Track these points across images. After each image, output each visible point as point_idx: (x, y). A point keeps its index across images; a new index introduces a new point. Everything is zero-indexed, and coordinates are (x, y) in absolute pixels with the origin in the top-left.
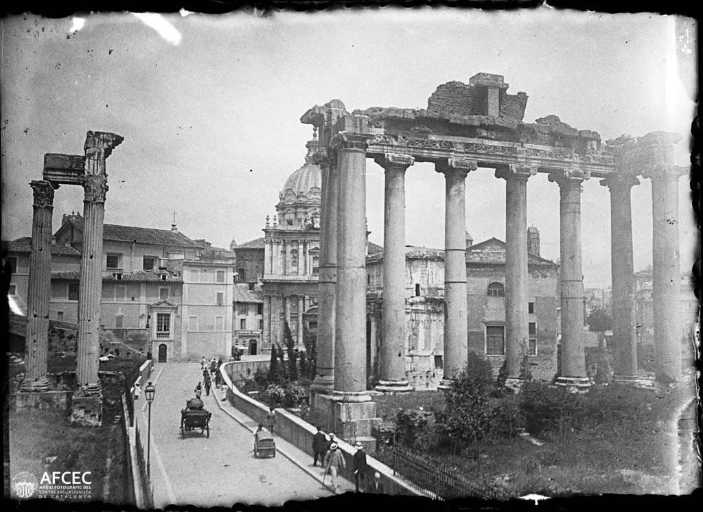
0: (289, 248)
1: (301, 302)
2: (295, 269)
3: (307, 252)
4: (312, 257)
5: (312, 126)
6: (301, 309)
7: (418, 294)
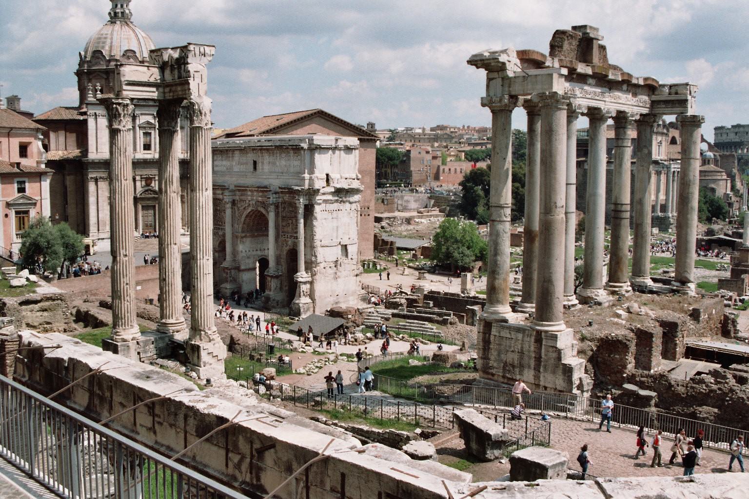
3: (137, 128)
4: (141, 132)
5: (483, 73)
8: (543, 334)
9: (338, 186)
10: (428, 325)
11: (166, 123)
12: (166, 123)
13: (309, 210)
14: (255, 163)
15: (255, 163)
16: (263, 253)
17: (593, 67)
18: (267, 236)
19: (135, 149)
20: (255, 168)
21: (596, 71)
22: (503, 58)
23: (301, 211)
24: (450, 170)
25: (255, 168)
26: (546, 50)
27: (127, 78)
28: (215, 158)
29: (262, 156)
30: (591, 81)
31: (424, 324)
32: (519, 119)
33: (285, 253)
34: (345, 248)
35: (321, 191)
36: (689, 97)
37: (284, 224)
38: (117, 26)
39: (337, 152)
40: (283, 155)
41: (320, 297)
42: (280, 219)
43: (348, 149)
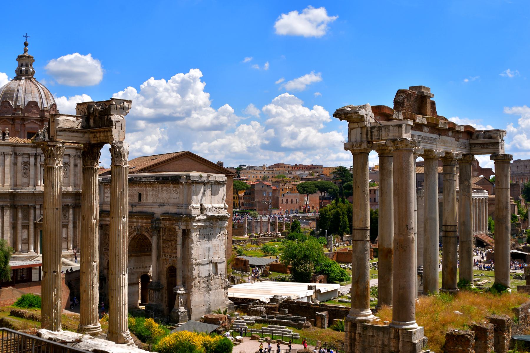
0: (20, 159)
1: (32, 211)
2: (25, 180)
3: (38, 165)
4: (42, 169)
5: (345, 124)
6: (32, 218)
7: (202, 213)
8: (400, 331)
9: (210, 214)
10: (287, 329)
11: (89, 162)
12: (89, 162)
13: (186, 234)
14: (140, 195)
15: (140, 195)
16: (145, 270)
17: (427, 118)
18: (150, 255)
19: (35, 185)
20: (140, 199)
21: (430, 121)
22: (362, 112)
23: (180, 233)
24: (287, 200)
25: (140, 199)
26: (392, 106)
27: (60, 126)
28: (106, 191)
29: (146, 190)
30: (426, 129)
31: (283, 328)
32: (374, 159)
33: (165, 269)
34: (216, 265)
35: (197, 218)
36: (500, 141)
37: (164, 246)
38: (23, 81)
39: (209, 185)
40: (165, 189)
41: (195, 306)
42: (161, 241)
43: (219, 183)
